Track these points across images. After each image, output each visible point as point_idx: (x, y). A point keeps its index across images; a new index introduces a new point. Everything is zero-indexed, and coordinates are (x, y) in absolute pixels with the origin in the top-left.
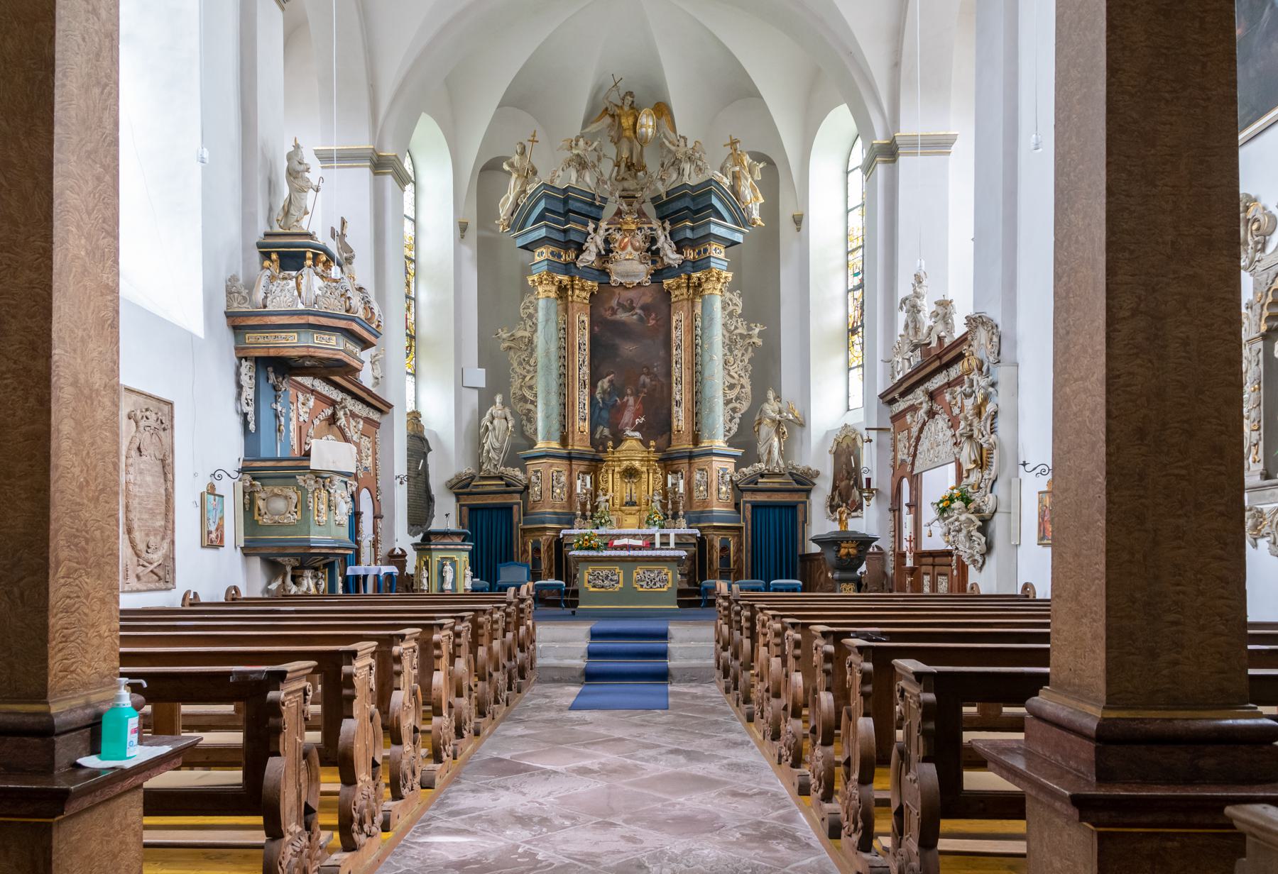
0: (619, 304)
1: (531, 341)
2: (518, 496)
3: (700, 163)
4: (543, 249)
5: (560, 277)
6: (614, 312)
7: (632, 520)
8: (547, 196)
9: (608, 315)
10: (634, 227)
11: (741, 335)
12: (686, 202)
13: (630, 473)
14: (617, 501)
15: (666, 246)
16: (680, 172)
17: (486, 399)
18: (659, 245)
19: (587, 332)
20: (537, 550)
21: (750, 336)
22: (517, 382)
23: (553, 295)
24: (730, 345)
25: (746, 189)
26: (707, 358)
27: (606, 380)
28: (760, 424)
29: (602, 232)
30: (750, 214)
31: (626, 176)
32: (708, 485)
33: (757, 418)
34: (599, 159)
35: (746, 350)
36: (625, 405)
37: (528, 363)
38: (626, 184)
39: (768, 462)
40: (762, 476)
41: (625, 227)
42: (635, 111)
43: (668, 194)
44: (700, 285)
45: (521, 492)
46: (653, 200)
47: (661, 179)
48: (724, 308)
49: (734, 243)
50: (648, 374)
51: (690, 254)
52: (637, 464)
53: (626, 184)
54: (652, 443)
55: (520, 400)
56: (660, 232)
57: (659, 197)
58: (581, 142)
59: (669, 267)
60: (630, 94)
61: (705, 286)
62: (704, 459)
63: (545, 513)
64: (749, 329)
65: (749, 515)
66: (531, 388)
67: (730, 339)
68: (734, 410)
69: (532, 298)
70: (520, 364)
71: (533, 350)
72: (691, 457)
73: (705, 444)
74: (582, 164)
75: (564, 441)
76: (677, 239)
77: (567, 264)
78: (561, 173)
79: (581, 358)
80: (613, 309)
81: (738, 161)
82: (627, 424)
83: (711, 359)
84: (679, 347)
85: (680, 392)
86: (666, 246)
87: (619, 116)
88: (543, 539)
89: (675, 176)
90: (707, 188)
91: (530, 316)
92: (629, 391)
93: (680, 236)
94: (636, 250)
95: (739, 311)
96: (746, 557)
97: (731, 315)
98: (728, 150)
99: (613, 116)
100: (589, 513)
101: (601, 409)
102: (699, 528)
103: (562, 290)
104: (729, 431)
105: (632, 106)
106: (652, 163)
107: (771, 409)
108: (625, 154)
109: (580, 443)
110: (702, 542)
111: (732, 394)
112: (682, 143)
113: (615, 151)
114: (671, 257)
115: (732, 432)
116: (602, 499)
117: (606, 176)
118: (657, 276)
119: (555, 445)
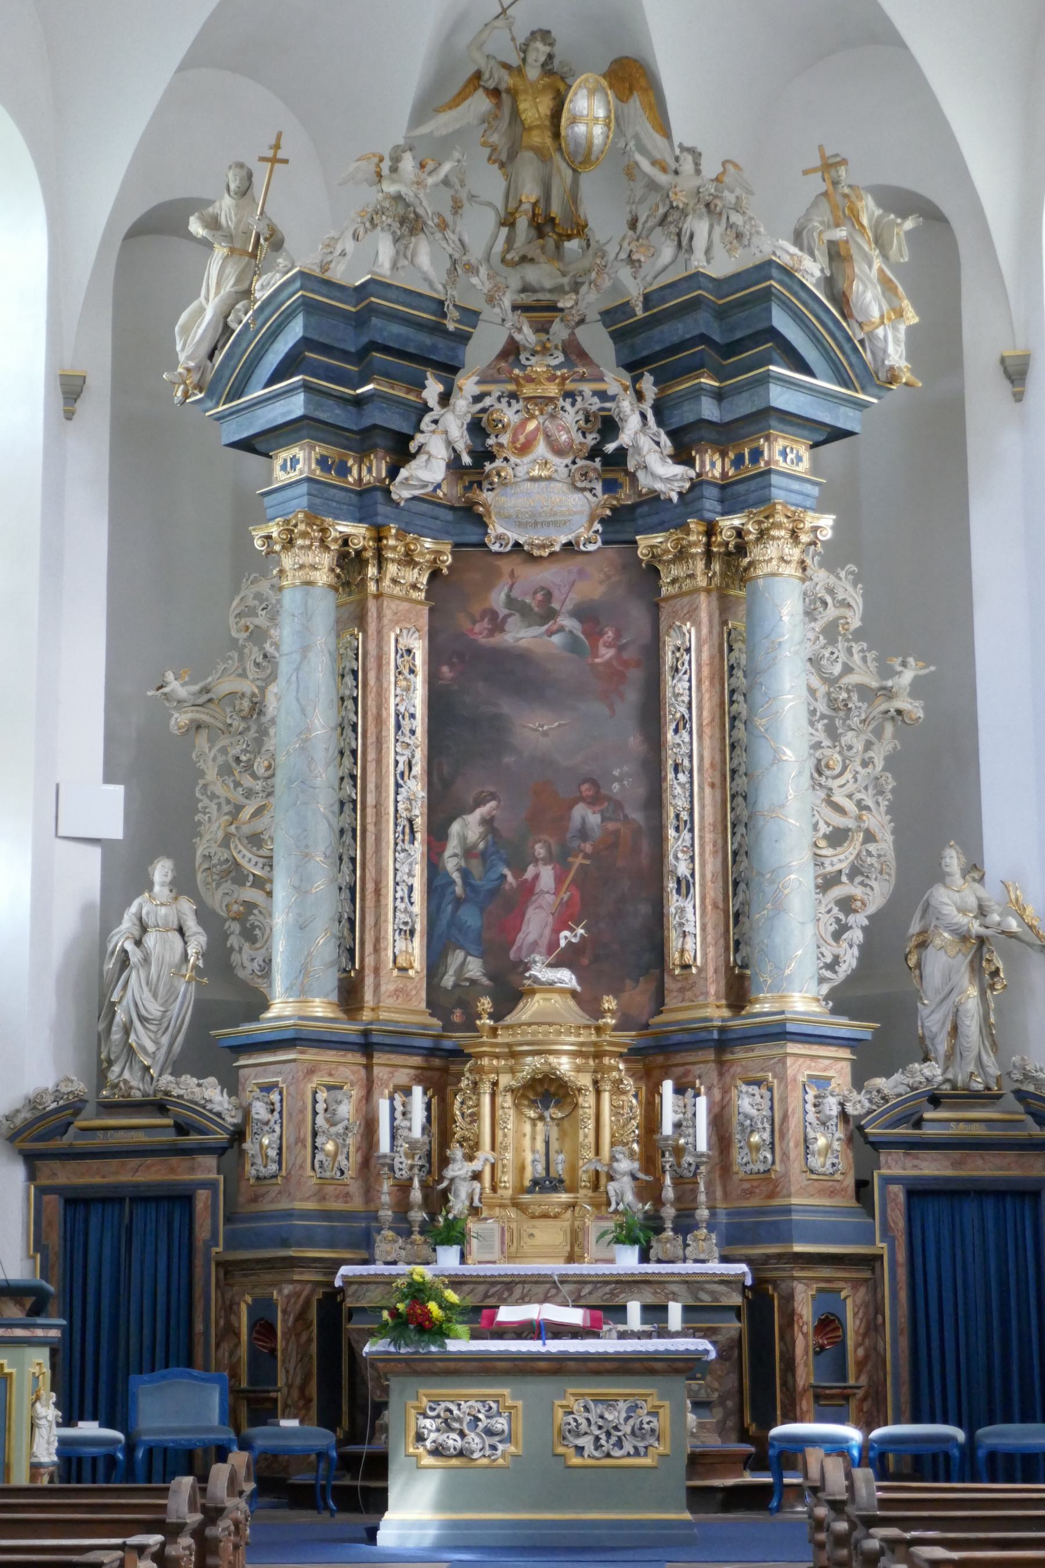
0: (511, 602)
1: (257, 707)
2: (211, 1161)
3: (736, 218)
4: (297, 451)
5: (345, 527)
6: (498, 625)
7: (550, 1235)
8: (308, 307)
9: (480, 633)
10: (552, 390)
11: (863, 691)
12: (702, 323)
13: (547, 1092)
14: (507, 1179)
15: (645, 443)
16: (683, 244)
17: (124, 875)
18: (625, 438)
19: (420, 682)
20: (263, 1328)
21: (888, 693)
22: (213, 827)
23: (322, 578)
24: (832, 716)
25: (868, 297)
26: (764, 754)
27: (474, 819)
28: (923, 945)
29: (462, 404)
30: (880, 354)
31: (533, 252)
32: (777, 1128)
33: (915, 927)
34: (457, 207)
35: (878, 732)
36: (528, 890)
37: (249, 767)
38: (532, 274)
39: (949, 1057)
40: (935, 1100)
41: (528, 390)
42: (557, 84)
43: (647, 299)
44: (741, 550)
45: (220, 1151)
46: (608, 316)
47: (630, 260)
48: (810, 614)
49: (837, 434)
50: (595, 801)
51: (713, 465)
52: (564, 1065)
54: (609, 1003)
55: (224, 875)
56: (626, 403)
58: (408, 164)
59: (654, 499)
60: (544, 35)
61: (756, 552)
62: (762, 1050)
63: (289, 1214)
64: (886, 671)
65: (898, 1220)
66: (256, 840)
67: (831, 702)
68: (846, 905)
69: (264, 587)
70: (225, 771)
71: (263, 733)
72: (724, 1043)
73: (763, 1006)
74: (409, 223)
75: (349, 994)
76: (676, 422)
77: (364, 493)
78: (349, 245)
79: (404, 754)
80: (493, 614)
82: (534, 947)
83: (777, 760)
84: (683, 723)
85: (690, 854)
86: (645, 443)
87: (513, 93)
88: (282, 1294)
89: (667, 252)
91: (258, 636)
92: (540, 850)
93: (685, 415)
94: (558, 451)
95: (856, 623)
96: (895, 1345)
97: (831, 632)
98: (817, 184)
99: (495, 93)
100: (418, 1215)
101: (458, 902)
102: (749, 1261)
103: (350, 564)
104: (832, 966)
105: (548, 67)
107: (953, 901)
108: (530, 193)
109: (398, 994)
110: (761, 1305)
111: (840, 859)
112: (687, 165)
113: (503, 184)
114: (661, 472)
115: (844, 970)
116: (459, 1169)
117: (476, 253)
118: (623, 521)
119: (321, 1008)
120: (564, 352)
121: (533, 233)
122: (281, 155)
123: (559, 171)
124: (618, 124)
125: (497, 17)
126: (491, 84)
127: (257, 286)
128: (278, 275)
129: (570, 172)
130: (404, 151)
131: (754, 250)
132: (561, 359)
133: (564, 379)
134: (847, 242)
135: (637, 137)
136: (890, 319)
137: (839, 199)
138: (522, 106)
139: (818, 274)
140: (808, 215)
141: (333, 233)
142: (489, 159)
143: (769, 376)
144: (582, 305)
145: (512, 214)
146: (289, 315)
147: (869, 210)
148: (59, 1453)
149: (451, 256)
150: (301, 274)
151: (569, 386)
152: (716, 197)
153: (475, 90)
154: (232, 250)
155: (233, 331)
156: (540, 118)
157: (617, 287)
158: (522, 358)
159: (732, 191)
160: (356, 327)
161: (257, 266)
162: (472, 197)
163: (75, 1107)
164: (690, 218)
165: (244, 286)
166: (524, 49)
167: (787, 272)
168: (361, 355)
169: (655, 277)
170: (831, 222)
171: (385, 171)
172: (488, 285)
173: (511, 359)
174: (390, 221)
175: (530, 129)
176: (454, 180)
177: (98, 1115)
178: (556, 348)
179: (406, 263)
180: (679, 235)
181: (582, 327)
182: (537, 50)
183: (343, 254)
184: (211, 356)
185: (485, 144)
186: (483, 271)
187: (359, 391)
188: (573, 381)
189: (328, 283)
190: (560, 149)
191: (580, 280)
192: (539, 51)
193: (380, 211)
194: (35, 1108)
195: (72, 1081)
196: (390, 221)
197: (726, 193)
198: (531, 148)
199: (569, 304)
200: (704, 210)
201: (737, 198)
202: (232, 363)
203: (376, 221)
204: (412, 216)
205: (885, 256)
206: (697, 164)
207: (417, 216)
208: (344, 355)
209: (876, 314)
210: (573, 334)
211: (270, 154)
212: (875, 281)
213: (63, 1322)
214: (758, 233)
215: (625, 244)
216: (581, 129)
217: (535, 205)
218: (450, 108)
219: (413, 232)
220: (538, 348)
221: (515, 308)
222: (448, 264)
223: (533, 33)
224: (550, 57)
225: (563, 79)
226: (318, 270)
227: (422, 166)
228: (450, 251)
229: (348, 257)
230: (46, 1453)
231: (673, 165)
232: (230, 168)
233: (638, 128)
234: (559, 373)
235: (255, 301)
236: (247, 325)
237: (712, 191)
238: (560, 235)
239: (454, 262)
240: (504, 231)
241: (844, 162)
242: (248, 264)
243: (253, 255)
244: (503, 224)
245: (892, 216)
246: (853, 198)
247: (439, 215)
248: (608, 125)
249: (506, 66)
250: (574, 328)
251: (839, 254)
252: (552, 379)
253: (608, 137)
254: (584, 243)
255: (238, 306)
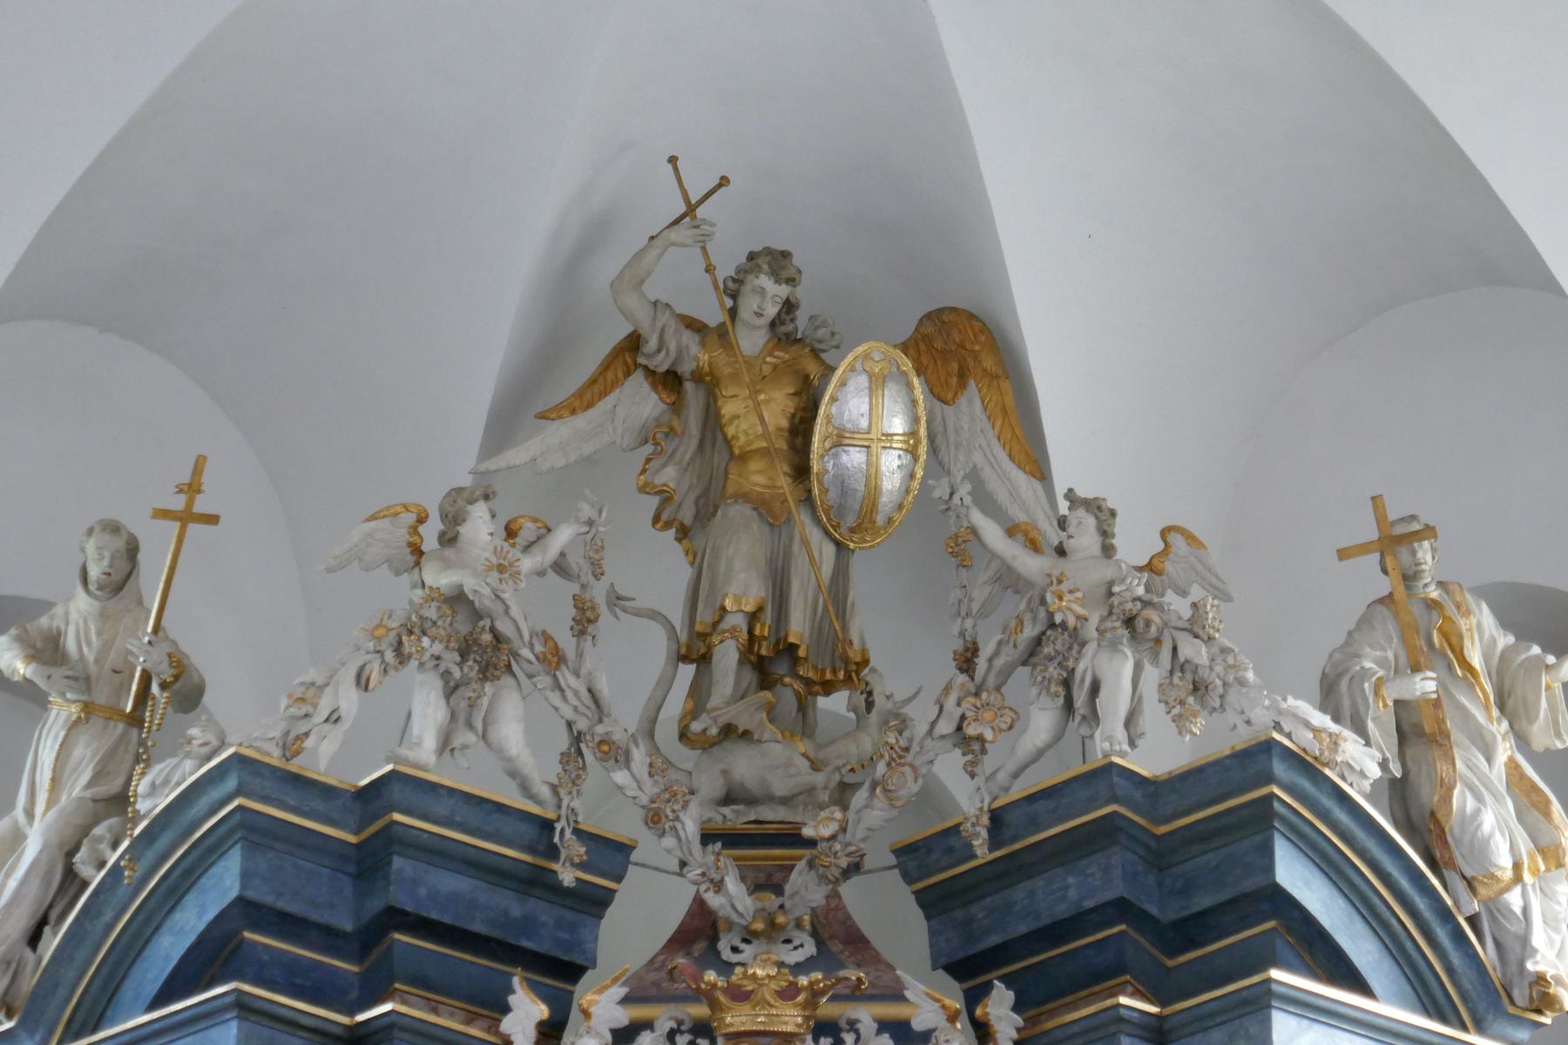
3: (1190, 649)
16: (1077, 703)
31: (747, 715)
34: (584, 621)
38: (745, 765)
43: (997, 819)
46: (913, 858)
47: (962, 739)
53: (745, 765)
57: (949, 840)
58: (480, 527)
60: (777, 262)
74: (479, 651)
78: (348, 699)
81: (1434, 645)
87: (708, 382)
89: (1042, 722)
90: (1242, 797)
98: (1370, 580)
99: (669, 381)
105: (782, 329)
106: (905, 655)
108: (743, 590)
112: (1085, 538)
113: (686, 573)
117: (625, 719)
120: (815, 934)
121: (750, 677)
122: (202, 505)
123: (805, 543)
124: (933, 449)
125: (677, 222)
126: (662, 363)
127: (143, 786)
128: (188, 764)
129: (829, 550)
130: (471, 502)
131: (1231, 717)
132: (810, 949)
133: (815, 993)
134: (1437, 703)
135: (974, 476)
136: (1535, 871)
137: (1417, 610)
138: (728, 409)
139: (1375, 772)
140: (1349, 649)
141: (312, 675)
142: (656, 519)
143: (1269, 993)
144: (857, 833)
145: (703, 636)
146: (211, 850)
147: (1483, 634)
149: (569, 724)
150: (238, 759)
151: (827, 1009)
152: (1147, 604)
153: (628, 374)
154: (88, 708)
155: (85, 884)
156: (765, 435)
157: (932, 795)
158: (724, 947)
159: (1183, 593)
160: (358, 877)
161: (142, 743)
162: (617, 600)
164: (1090, 649)
165: (113, 786)
166: (733, 290)
167: (1306, 766)
168: (367, 939)
169: (1016, 775)
170: (1403, 661)
171: (430, 542)
172: (651, 788)
173: (699, 947)
174: (438, 648)
175: (744, 457)
176: (576, 561)
178: (799, 925)
179: (470, 738)
180: (1067, 684)
181: (855, 880)
182: (762, 292)
183: (334, 718)
184: (34, 939)
185: (643, 489)
186: (639, 756)
187: (361, 1017)
188: (834, 998)
189: (299, 781)
190: (808, 500)
191: (850, 779)
192: (767, 294)
193: (416, 627)
196: (438, 648)
197: (1170, 597)
198: (744, 497)
199: (826, 831)
200: (1124, 633)
201: (1194, 605)
202: (80, 955)
203: (407, 649)
204: (487, 637)
205: (1522, 741)
206: (1105, 534)
207: (498, 638)
208: (329, 938)
209: (1504, 861)
210: (835, 895)
211: (178, 503)
212: (1502, 789)
214: (1242, 682)
215: (950, 702)
216: (854, 458)
217: (753, 617)
218: (573, 412)
219: (487, 672)
220: (759, 926)
221: (707, 838)
222: (563, 742)
223: (752, 257)
224: (789, 306)
225: (816, 353)
226: (277, 753)
227: (511, 533)
228: (567, 712)
229: (345, 725)
231: (1054, 536)
232: (90, 532)
233: (978, 458)
234: (803, 981)
235: (135, 820)
236: (116, 870)
237: (1141, 591)
238: (808, 682)
239: (577, 739)
240: (687, 671)
241: (1429, 532)
242: (123, 738)
243: (135, 719)
244: (684, 658)
245: (1536, 650)
246: (1451, 610)
247: (547, 637)
248: (913, 452)
249: (694, 325)
250: (836, 882)
251: (1420, 733)
252: (788, 993)
253: (912, 476)
254: (861, 700)
255: (98, 831)
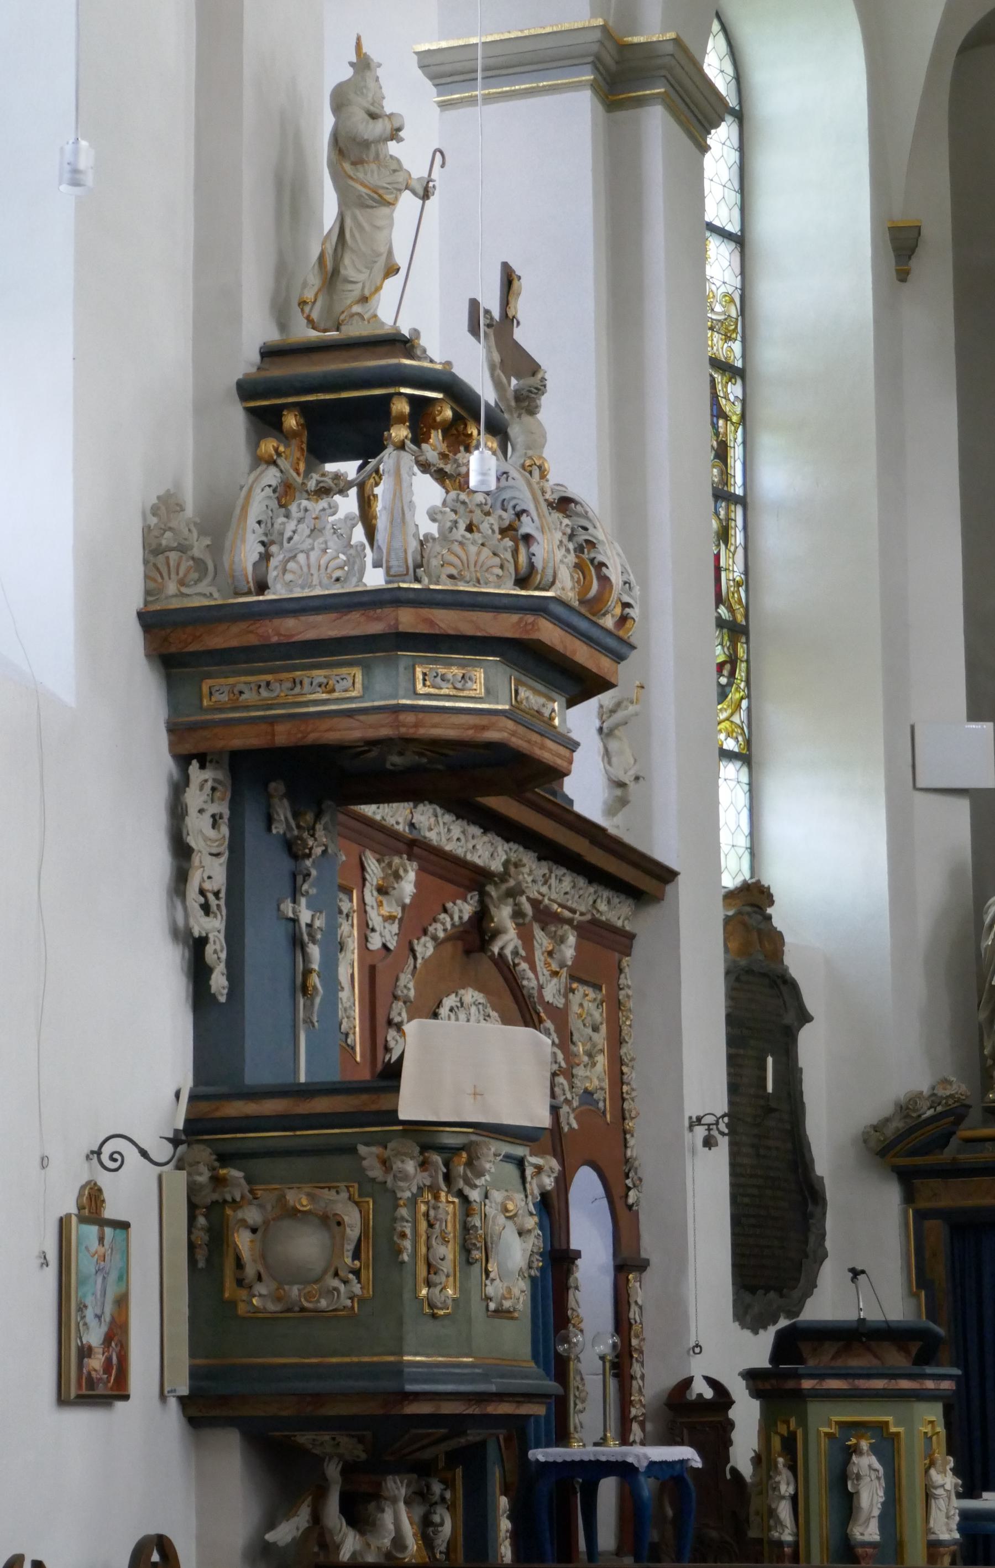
148: (960, 1528)
163: (955, 1113)
177: (985, 1123)
194: (907, 1116)
195: (951, 1083)
213: (959, 1372)
230: (946, 1529)
